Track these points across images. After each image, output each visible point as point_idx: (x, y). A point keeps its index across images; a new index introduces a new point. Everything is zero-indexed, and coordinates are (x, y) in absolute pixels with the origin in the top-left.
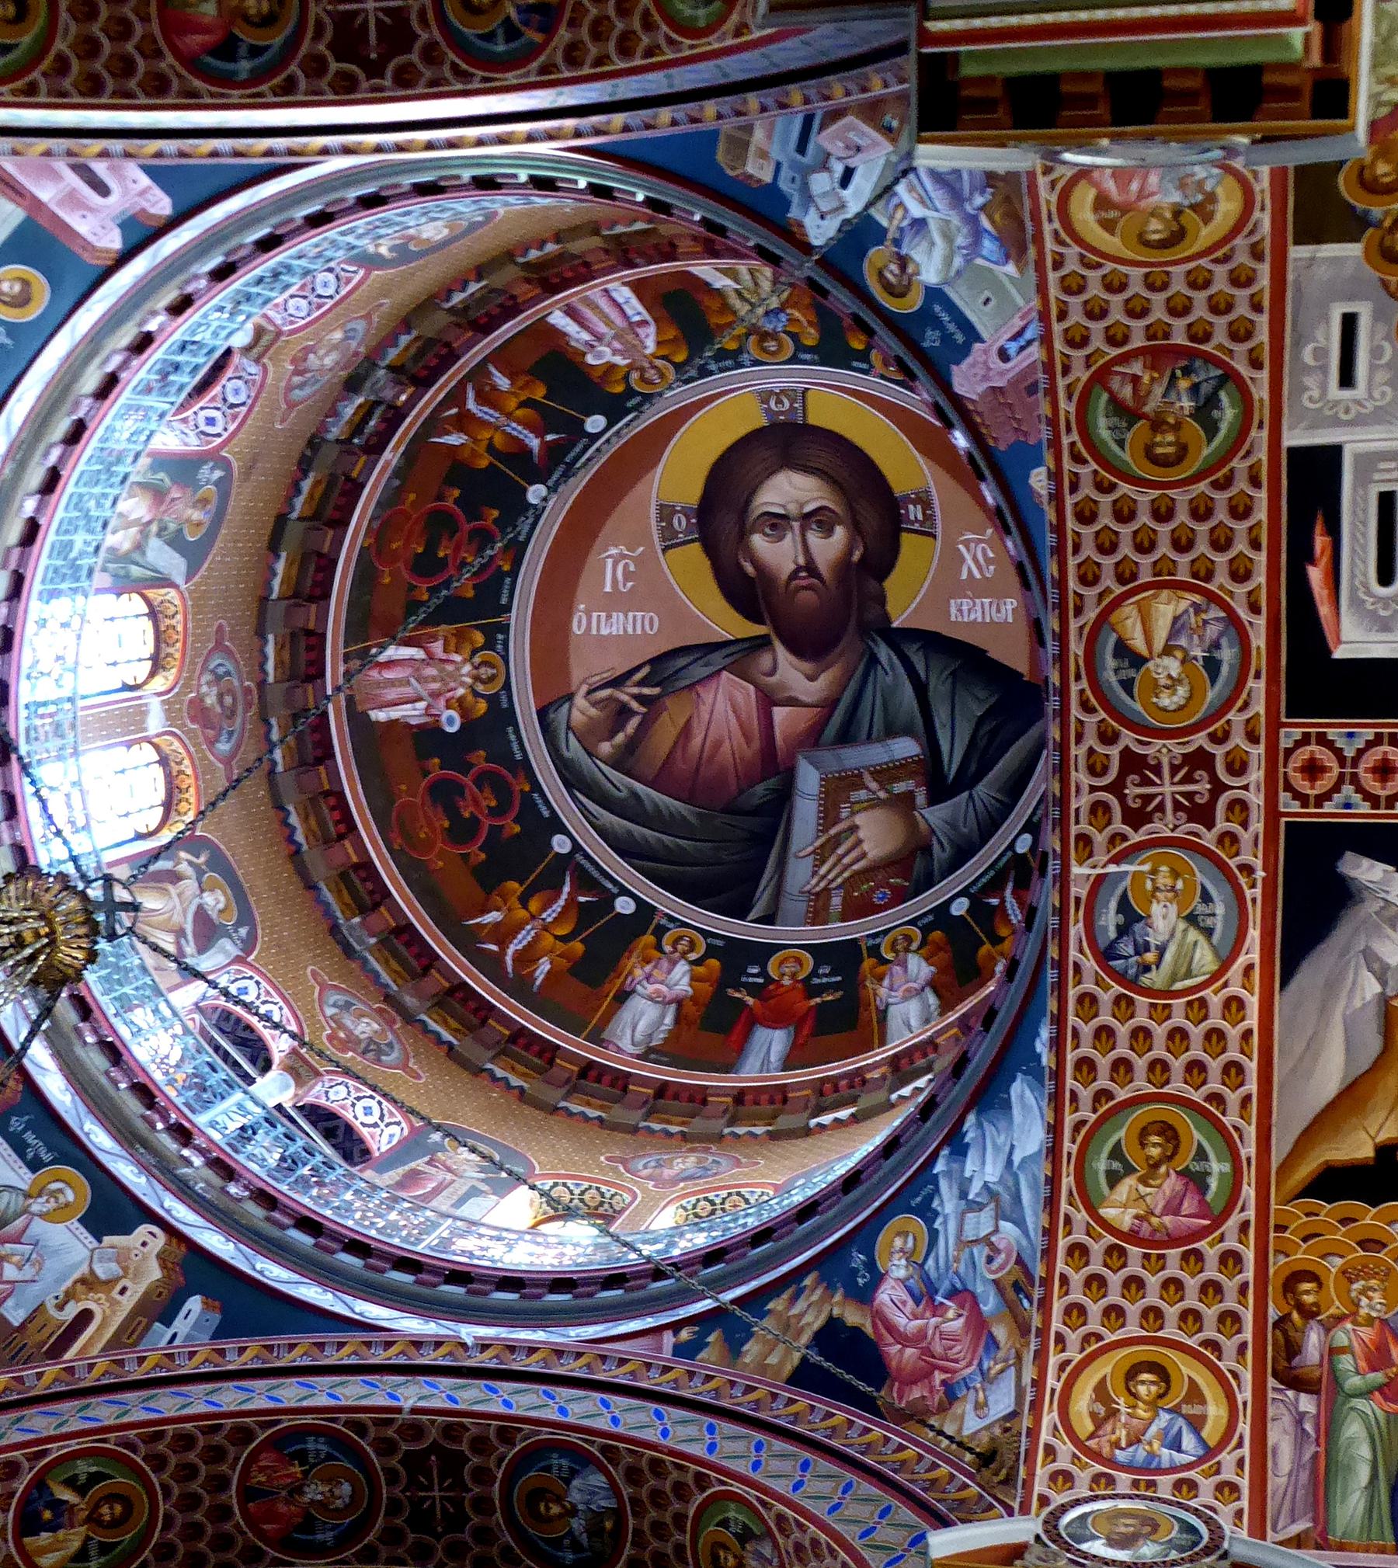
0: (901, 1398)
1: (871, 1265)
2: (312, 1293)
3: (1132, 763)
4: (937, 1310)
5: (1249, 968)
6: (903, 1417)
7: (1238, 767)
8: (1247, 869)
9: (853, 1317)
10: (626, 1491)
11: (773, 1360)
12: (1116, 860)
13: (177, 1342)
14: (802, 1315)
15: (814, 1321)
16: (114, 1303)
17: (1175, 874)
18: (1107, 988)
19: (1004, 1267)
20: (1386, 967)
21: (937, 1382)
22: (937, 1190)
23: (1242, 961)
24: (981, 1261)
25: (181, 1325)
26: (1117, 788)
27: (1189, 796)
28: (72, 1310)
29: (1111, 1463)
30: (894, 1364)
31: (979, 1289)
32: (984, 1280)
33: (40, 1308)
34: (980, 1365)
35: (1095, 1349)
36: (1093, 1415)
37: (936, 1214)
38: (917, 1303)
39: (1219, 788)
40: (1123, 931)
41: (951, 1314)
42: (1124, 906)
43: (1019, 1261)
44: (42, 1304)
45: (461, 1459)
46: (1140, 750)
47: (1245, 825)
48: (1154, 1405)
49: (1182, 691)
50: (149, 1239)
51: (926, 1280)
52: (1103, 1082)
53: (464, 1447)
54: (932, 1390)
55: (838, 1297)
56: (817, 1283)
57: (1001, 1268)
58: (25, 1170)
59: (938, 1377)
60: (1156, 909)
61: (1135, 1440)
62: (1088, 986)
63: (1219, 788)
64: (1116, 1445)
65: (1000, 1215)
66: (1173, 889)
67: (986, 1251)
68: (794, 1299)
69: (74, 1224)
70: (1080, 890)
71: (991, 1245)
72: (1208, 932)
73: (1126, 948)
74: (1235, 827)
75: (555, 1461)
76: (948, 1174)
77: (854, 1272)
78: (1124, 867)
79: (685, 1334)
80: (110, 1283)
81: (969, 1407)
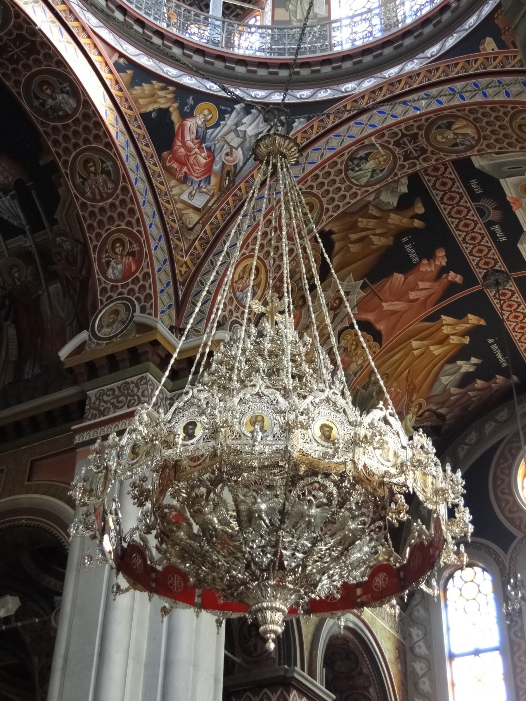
0: (170, 162)
1: (193, 108)
3: (415, 137)
4: (200, 148)
5: (367, 191)
6: (169, 170)
7: (425, 160)
8: (396, 174)
9: (175, 117)
10: (78, 115)
11: (141, 101)
12: (381, 145)
14: (161, 97)
17: (385, 160)
18: (341, 165)
19: (230, 165)
20: (379, 198)
21: (184, 171)
22: (231, 113)
23: (368, 188)
26: (404, 135)
27: (411, 152)
29: (235, 294)
30: (175, 148)
31: (217, 159)
32: (221, 158)
34: (200, 182)
37: (224, 120)
38: (197, 138)
39: (417, 158)
40: (361, 158)
41: (203, 155)
42: (368, 155)
43: (235, 166)
45: (38, 53)
46: (419, 136)
47: (409, 168)
49: (444, 140)
51: (205, 134)
52: (314, 184)
53: (42, 52)
54: (181, 170)
55: (176, 105)
56: (174, 92)
57: (228, 161)
59: (185, 169)
60: (371, 162)
61: (242, 291)
62: (339, 161)
63: (417, 158)
65: (241, 145)
66: (380, 162)
67: (229, 150)
68: (163, 89)
70: (367, 142)
71: (231, 151)
72: (372, 176)
73: (356, 162)
74: (407, 167)
75: (66, 84)
76: (238, 113)
77: (187, 104)
78: (380, 148)
79: (122, 61)
81: (188, 191)
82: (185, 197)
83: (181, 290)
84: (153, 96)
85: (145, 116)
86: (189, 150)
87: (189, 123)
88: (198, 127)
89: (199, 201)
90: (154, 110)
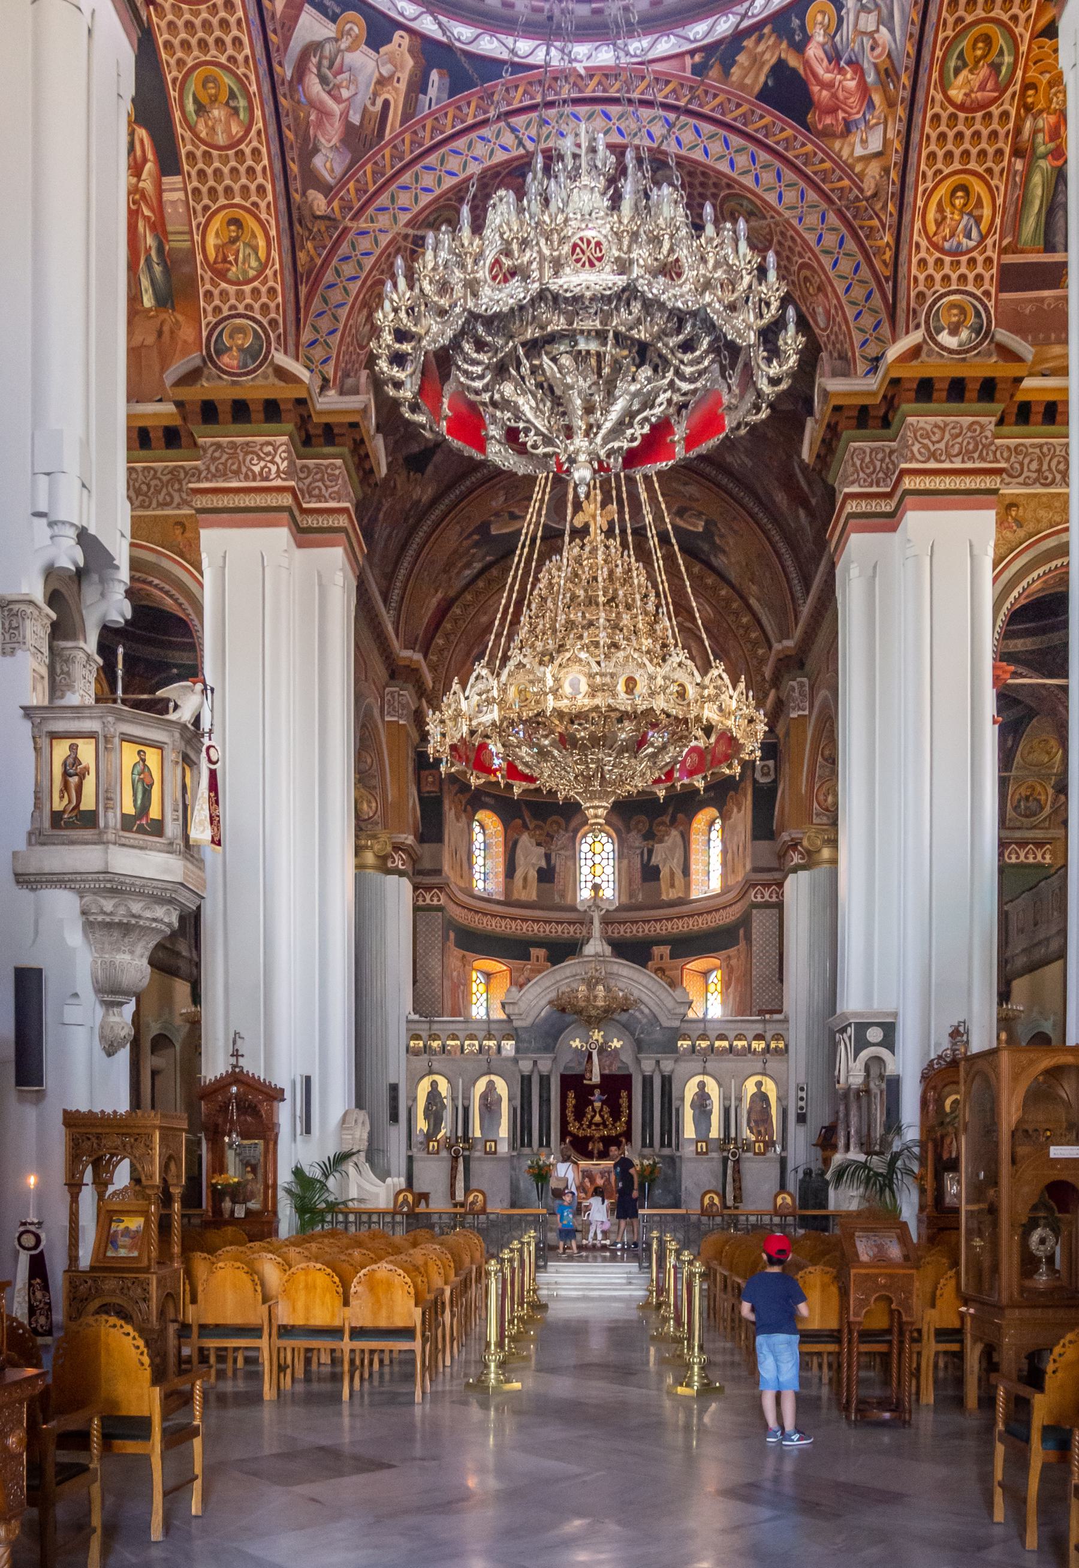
0: (820, 120)
1: (803, 27)
2: (489, 46)
4: (841, 71)
9: (793, 61)
11: (748, 81)
13: (434, 108)
14: (764, 53)
15: (770, 59)
16: (396, 90)
24: (867, 47)
25: (432, 92)
28: (379, 102)
30: (816, 98)
31: (866, 66)
33: (365, 110)
35: (940, 178)
36: (936, 221)
38: (830, 62)
41: (849, 76)
44: (365, 107)
48: (962, 213)
50: (400, 41)
51: (834, 46)
55: (784, 46)
56: (773, 31)
58: (331, 25)
61: (952, 235)
64: (945, 239)
68: (758, 41)
69: (364, 47)
80: (391, 77)
81: (858, 140)
82: (859, 151)
83: (888, 287)
84: (755, 60)
85: (764, 95)
86: (829, 86)
87: (813, 51)
88: (823, 45)
89: (875, 144)
90: (767, 77)
